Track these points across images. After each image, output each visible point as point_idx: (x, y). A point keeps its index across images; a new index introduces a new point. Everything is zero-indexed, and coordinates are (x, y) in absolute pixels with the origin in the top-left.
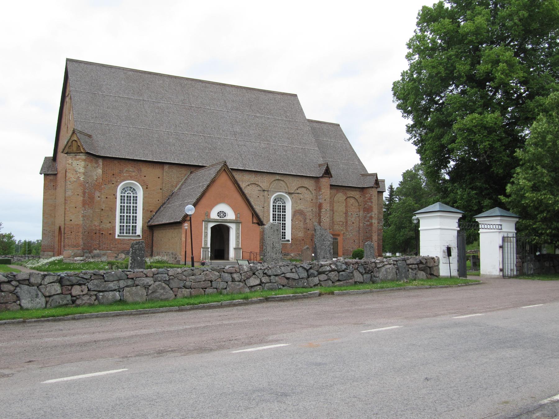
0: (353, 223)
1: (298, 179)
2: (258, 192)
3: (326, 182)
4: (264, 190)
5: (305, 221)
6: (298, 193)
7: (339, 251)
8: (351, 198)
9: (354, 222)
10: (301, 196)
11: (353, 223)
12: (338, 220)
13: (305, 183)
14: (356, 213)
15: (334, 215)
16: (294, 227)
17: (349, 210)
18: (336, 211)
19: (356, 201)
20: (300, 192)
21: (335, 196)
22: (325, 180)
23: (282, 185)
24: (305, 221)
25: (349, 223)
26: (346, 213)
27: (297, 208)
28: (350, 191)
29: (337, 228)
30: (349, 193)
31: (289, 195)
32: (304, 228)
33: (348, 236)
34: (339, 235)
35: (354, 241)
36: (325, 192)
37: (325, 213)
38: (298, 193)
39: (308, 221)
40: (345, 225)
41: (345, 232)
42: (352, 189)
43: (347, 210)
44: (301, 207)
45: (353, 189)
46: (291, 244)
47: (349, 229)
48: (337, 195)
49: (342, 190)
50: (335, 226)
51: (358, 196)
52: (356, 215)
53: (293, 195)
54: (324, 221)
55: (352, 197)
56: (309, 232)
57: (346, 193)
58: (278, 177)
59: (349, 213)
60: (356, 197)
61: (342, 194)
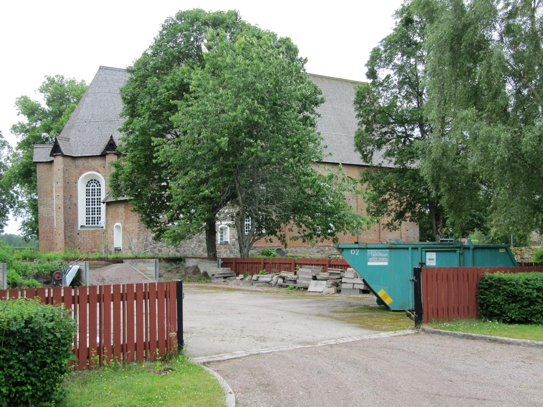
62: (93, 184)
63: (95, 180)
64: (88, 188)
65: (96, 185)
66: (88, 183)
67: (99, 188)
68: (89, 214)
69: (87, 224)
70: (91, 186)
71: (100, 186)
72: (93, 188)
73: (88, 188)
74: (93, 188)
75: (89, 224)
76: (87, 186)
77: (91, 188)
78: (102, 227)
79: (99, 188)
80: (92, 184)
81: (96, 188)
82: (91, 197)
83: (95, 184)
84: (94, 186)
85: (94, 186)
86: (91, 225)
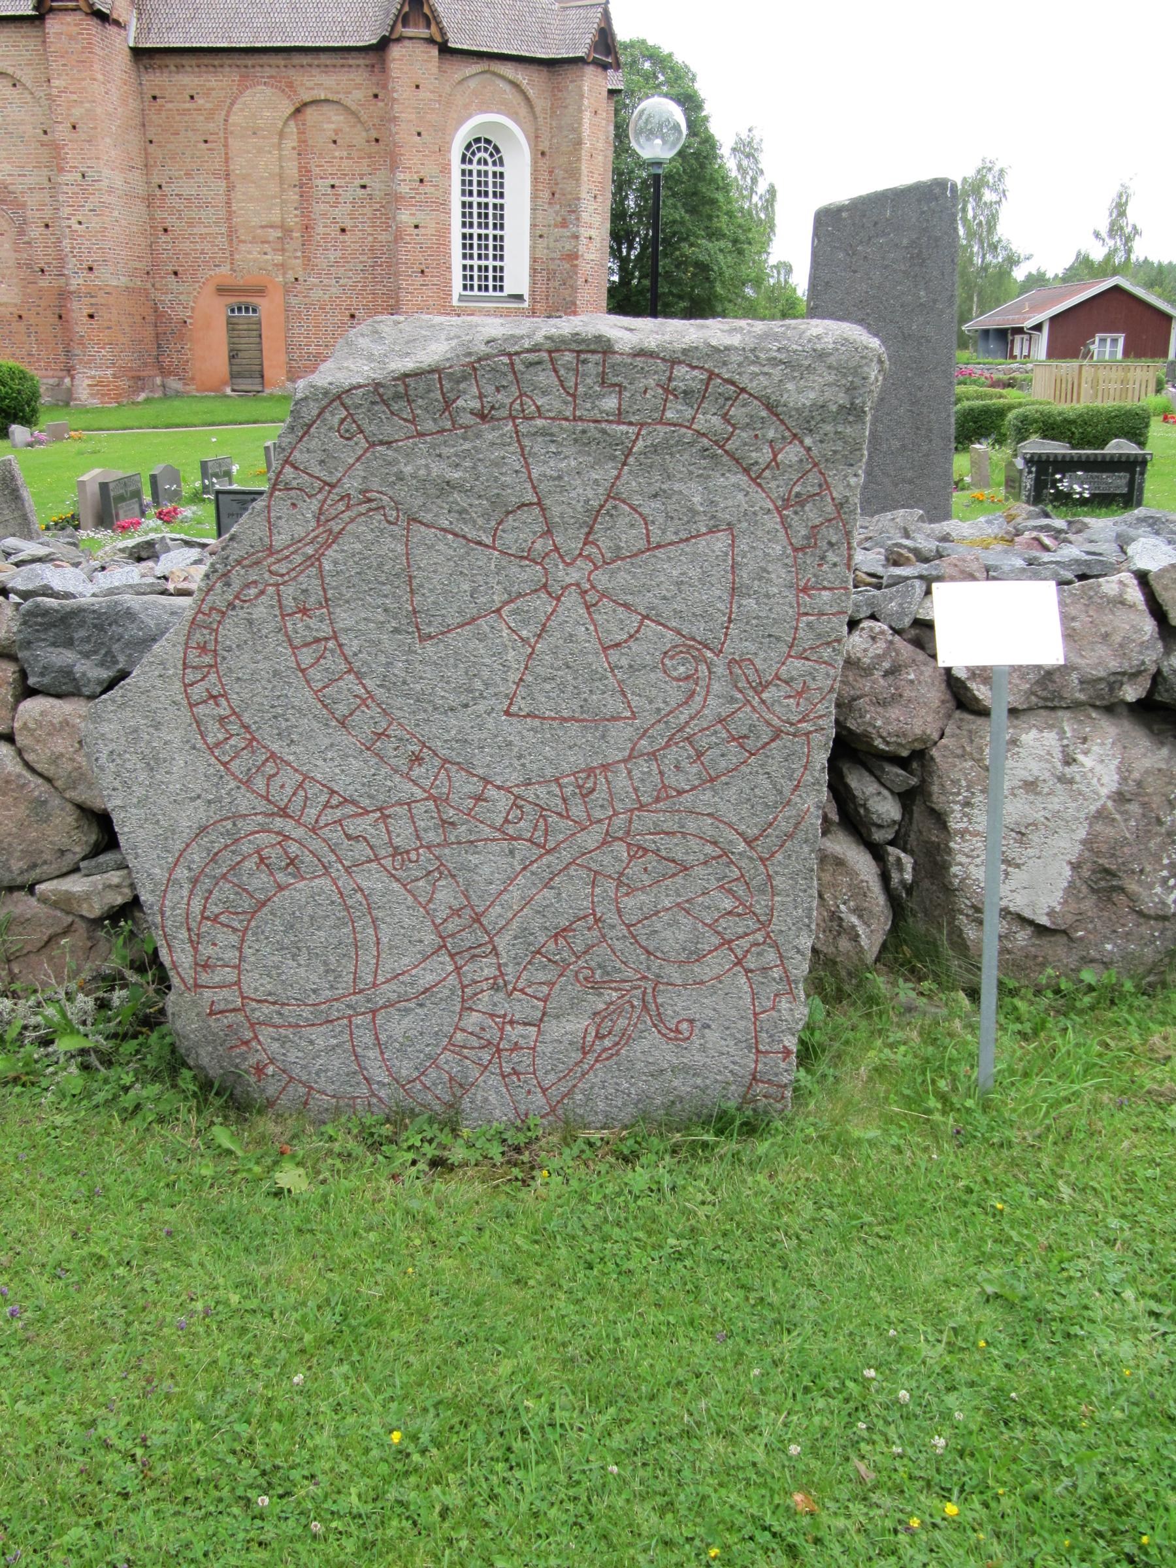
0: (343, 230)
3: (71, 38)
5: (22, 232)
7: (266, 363)
8: (326, 108)
9: (348, 224)
11: (343, 230)
12: (255, 221)
14: (358, 182)
15: (238, 195)
19: (353, 120)
21: (232, 104)
22: (65, 28)
24: (22, 232)
25: (320, 230)
26: (304, 186)
28: (315, 71)
29: (255, 255)
30: (309, 84)
32: (19, 265)
33: (317, 294)
34: (260, 291)
36: (72, 88)
37: (76, 189)
39: (35, 232)
40: (300, 241)
41: (300, 275)
42: (324, 59)
43: (305, 171)
45: (328, 62)
48: (247, 97)
49: (269, 71)
50: (243, 247)
51: (358, 95)
54: (76, 227)
55: (327, 101)
56: (42, 284)
57: (290, 85)
59: (319, 182)
60: (348, 102)
61: (269, 91)
62: (482, 155)
63: (488, 141)
65: (490, 161)
71: (502, 164)
72: (482, 168)
74: (482, 168)
75: (487, 288)
78: (519, 297)
79: (498, 169)
80: (478, 155)
83: (487, 156)
84: (486, 163)
85: (486, 163)
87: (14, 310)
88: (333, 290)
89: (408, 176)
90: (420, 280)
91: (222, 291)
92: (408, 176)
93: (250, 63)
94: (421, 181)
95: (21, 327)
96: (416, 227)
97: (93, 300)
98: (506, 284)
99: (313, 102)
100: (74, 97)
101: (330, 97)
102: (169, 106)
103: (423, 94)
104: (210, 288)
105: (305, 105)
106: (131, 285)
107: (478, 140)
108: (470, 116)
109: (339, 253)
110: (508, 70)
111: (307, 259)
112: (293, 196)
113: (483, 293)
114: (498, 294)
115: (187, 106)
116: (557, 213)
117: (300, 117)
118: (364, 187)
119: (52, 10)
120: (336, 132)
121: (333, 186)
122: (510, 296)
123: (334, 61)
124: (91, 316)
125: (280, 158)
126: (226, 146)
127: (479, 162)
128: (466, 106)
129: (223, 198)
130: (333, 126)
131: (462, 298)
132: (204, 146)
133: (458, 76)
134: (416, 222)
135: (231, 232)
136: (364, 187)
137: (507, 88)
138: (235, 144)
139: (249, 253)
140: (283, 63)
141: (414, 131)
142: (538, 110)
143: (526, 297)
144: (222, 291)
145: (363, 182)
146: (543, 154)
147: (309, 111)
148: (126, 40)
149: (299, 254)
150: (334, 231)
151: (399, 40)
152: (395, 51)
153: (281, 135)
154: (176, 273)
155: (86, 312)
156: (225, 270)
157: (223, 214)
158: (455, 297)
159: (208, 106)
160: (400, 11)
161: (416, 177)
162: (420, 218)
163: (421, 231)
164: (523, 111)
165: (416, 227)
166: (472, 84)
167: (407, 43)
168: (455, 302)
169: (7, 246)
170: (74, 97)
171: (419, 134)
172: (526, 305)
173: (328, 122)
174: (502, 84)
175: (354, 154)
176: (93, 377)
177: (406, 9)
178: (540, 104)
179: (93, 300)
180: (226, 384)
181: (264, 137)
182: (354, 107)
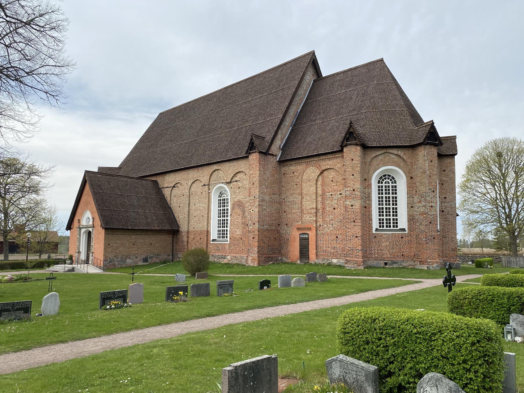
1: (234, 164)
2: (201, 188)
4: (204, 185)
6: (236, 181)
8: (330, 170)
9: (336, 206)
10: (240, 184)
13: (242, 166)
14: (339, 193)
16: (232, 223)
17: (327, 190)
18: (306, 194)
20: (239, 179)
23: (221, 176)
24: (244, 214)
25: (328, 209)
27: (236, 200)
29: (308, 218)
30: (325, 164)
31: (227, 185)
33: (326, 230)
35: (337, 237)
38: (236, 181)
42: (329, 156)
43: (323, 191)
44: (240, 197)
46: (229, 244)
47: (328, 219)
50: (305, 216)
52: (340, 196)
53: (231, 185)
54: (252, 212)
57: (319, 165)
58: (215, 167)
59: (327, 194)
60: (336, 168)
62: (387, 180)
64: (380, 185)
65: (390, 182)
66: (381, 177)
67: (394, 184)
68: (383, 216)
69: (380, 227)
70: (384, 182)
71: (395, 183)
72: (387, 185)
73: (380, 185)
74: (387, 185)
76: (379, 183)
77: (384, 184)
78: (404, 230)
79: (394, 184)
80: (385, 181)
81: (391, 184)
82: (384, 195)
83: (389, 180)
84: (389, 183)
85: (389, 183)
86: (392, 228)
87: (239, 236)
88: (331, 228)
89: (349, 189)
90: (353, 224)
91: (298, 229)
92: (349, 189)
93: (309, 161)
94: (354, 190)
95: (241, 241)
96: (352, 206)
97: (254, 233)
98: (398, 225)
99: (326, 170)
100: (254, 176)
101: (330, 167)
102: (288, 176)
103: (354, 162)
104: (295, 229)
105: (324, 171)
106: (270, 228)
107: (385, 175)
108: (380, 168)
109: (333, 216)
110: (395, 151)
111: (323, 219)
112: (320, 199)
113: (388, 228)
114: (395, 228)
115: (292, 175)
116: (418, 198)
117: (323, 174)
118: (341, 194)
119: (250, 153)
120: (333, 178)
121: (331, 195)
122: (400, 229)
123: (332, 156)
124: (253, 238)
125: (316, 188)
126: (301, 185)
127: (386, 183)
128: (378, 165)
129: (300, 202)
130: (332, 176)
131: (377, 230)
132: (296, 186)
133: (374, 155)
134: (351, 204)
135: (302, 211)
136: (341, 194)
137: (395, 157)
138: (304, 185)
139: (307, 217)
140: (317, 159)
141: (351, 174)
142: (408, 163)
143: (407, 229)
144: (298, 229)
145: (340, 193)
146: (412, 178)
147: (325, 172)
148: (276, 159)
149: (321, 217)
150: (331, 209)
151: (346, 146)
152: (345, 150)
153: (317, 180)
154: (287, 224)
155: (252, 237)
156: (300, 223)
157: (300, 206)
158: (374, 229)
159: (297, 174)
160: (345, 137)
161: (351, 189)
162: (353, 202)
163: (354, 207)
164: (402, 164)
165: (352, 206)
166: (380, 157)
167: (349, 147)
168: (374, 232)
169: (240, 218)
170: (254, 176)
171: (353, 175)
172: (407, 232)
173: (330, 175)
174: (392, 156)
175: (338, 184)
176: (252, 257)
177: (348, 136)
178: (409, 161)
179: (254, 233)
180: (298, 259)
181: (312, 182)
182: (338, 169)
